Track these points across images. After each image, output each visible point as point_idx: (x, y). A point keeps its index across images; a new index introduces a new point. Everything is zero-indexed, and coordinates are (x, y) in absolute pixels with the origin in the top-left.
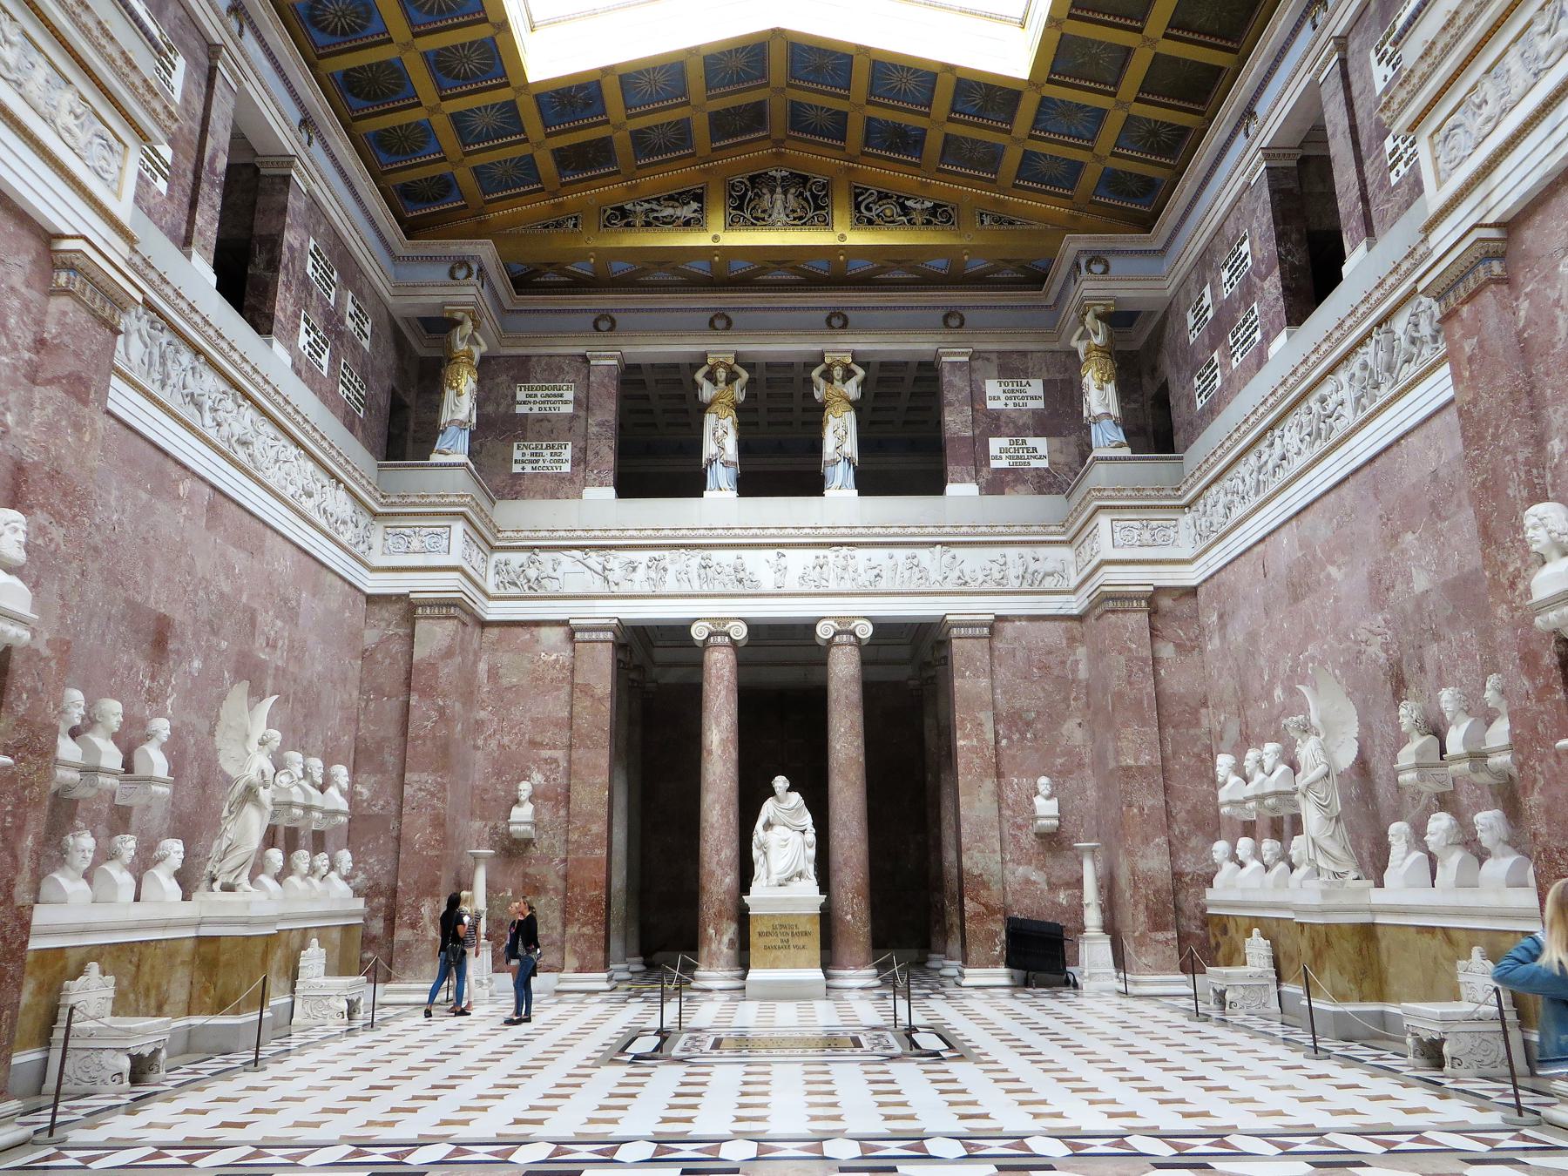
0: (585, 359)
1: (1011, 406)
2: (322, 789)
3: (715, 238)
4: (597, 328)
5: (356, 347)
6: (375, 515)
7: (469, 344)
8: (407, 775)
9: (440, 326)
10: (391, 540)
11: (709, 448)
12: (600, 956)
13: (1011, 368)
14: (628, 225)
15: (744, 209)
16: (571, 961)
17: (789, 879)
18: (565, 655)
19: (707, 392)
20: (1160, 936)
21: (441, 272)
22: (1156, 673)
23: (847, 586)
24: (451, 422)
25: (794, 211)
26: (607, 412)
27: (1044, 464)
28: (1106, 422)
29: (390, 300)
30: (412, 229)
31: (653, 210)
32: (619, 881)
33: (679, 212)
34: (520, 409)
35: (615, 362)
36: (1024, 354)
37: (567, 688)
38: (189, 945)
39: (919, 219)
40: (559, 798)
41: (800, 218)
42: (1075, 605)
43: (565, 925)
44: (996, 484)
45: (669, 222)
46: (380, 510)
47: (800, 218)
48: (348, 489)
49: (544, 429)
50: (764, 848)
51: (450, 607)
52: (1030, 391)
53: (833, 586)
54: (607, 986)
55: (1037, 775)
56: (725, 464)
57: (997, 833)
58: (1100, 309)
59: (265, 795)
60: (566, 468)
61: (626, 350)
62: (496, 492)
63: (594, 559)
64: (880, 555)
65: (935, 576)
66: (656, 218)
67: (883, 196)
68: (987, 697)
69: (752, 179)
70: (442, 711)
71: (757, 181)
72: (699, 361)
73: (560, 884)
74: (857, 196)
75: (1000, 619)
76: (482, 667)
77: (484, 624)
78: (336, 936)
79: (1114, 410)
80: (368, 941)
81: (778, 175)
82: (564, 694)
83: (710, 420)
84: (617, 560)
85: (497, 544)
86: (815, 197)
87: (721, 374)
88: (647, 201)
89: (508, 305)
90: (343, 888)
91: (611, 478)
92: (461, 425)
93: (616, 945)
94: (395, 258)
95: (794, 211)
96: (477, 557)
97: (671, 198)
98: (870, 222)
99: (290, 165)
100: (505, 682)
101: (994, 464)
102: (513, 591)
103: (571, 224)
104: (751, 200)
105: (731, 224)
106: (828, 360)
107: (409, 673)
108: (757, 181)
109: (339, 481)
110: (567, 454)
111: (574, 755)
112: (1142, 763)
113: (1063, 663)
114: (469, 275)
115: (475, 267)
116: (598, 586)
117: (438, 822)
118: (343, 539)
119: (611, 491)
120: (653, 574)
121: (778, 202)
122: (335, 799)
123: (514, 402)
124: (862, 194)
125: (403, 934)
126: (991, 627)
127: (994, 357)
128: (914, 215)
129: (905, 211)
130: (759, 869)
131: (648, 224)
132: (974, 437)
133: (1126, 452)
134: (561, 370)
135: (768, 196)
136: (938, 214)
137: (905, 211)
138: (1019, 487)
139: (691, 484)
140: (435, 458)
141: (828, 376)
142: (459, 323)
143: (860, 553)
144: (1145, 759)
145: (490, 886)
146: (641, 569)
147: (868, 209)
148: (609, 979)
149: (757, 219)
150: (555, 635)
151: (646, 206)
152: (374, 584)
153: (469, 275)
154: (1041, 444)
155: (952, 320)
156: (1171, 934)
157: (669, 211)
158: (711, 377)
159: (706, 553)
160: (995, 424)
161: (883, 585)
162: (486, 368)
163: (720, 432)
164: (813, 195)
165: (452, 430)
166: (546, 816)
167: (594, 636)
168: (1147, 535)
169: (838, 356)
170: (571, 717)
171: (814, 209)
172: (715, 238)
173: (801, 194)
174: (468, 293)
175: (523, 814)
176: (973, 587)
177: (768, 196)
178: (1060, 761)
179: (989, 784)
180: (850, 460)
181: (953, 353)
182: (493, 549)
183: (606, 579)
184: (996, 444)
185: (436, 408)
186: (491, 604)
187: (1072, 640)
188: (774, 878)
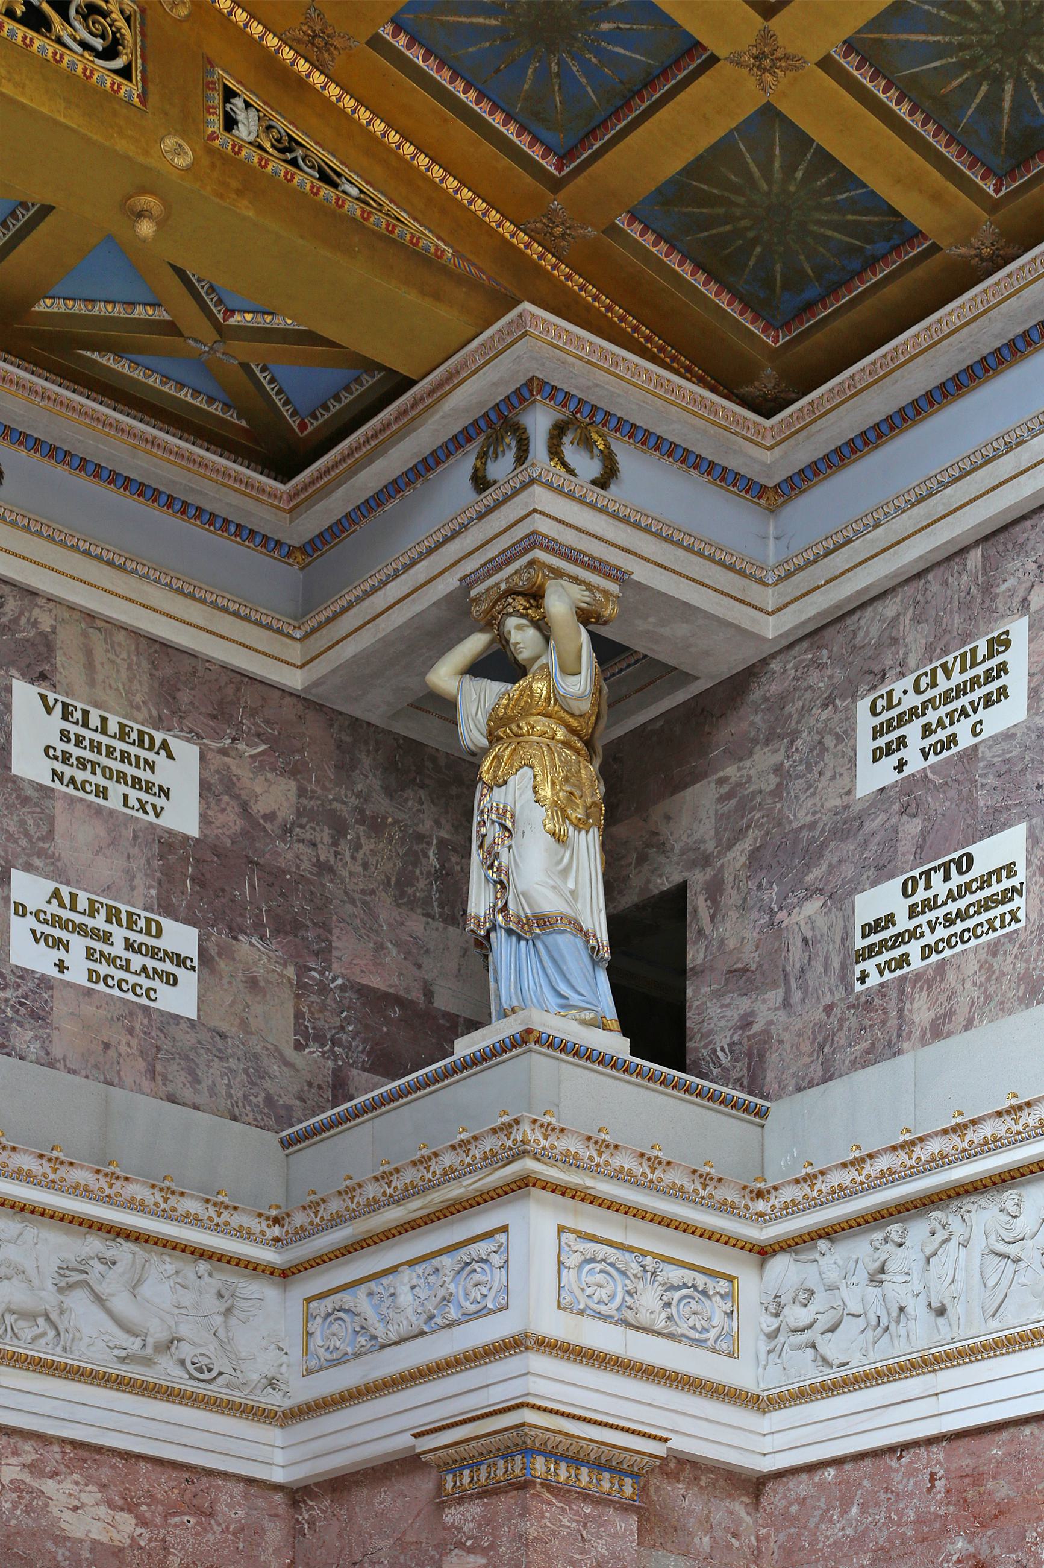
42: (279, 1457)
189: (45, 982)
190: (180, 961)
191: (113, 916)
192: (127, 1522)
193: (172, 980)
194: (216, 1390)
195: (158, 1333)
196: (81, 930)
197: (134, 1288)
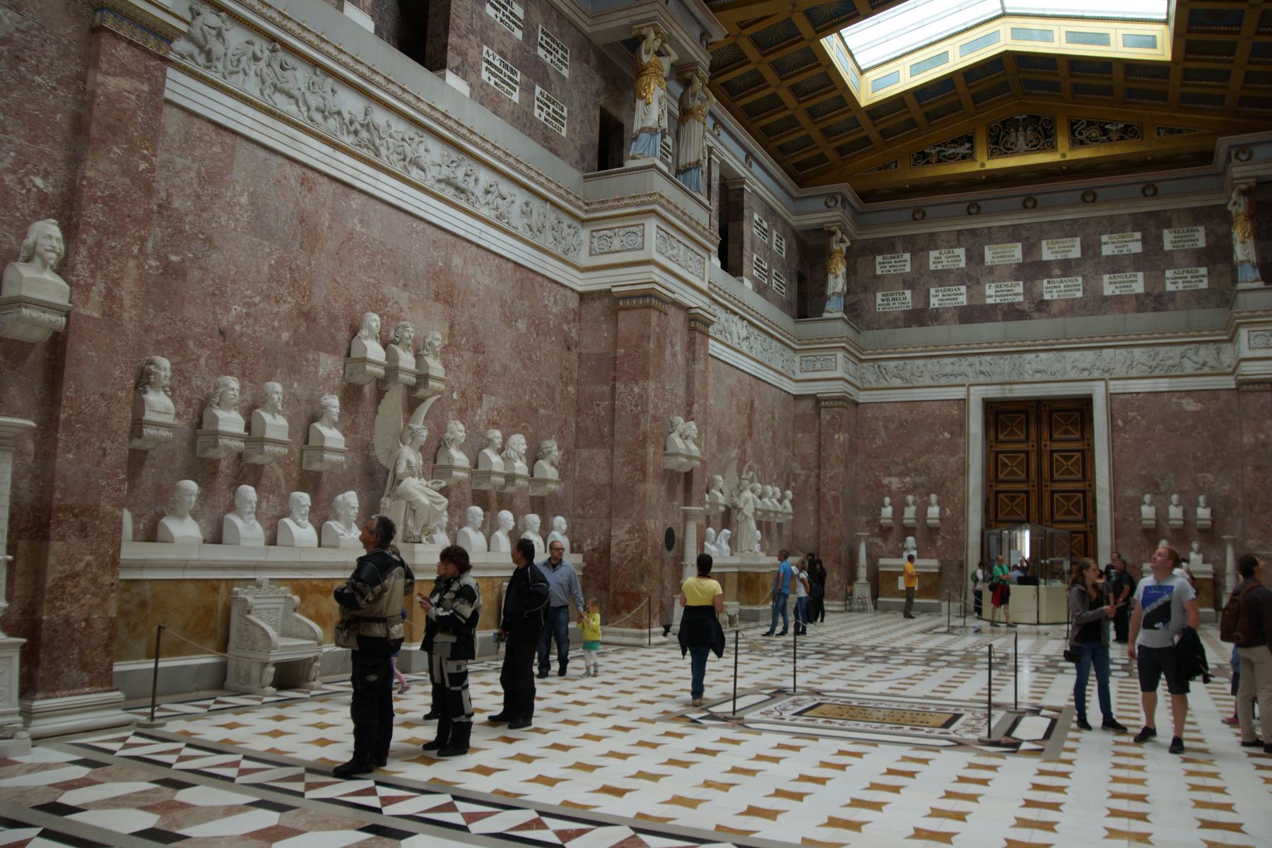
2: (760, 498)
3: (983, 165)
4: (915, 219)
7: (839, 246)
9: (824, 233)
14: (928, 163)
15: (999, 146)
21: (820, 203)
24: (833, 294)
25: (1031, 141)
28: (1247, 265)
29: (794, 224)
30: (801, 183)
31: (942, 151)
39: (1113, 136)
41: (1036, 146)
45: (952, 158)
46: (797, 347)
47: (1036, 146)
66: (944, 156)
67: (1090, 124)
69: (1003, 123)
71: (1008, 124)
74: (1072, 125)
79: (1253, 258)
81: (1020, 118)
85: (864, 357)
88: (939, 146)
92: (839, 295)
94: (794, 199)
95: (1031, 141)
96: (851, 366)
97: (953, 142)
98: (1082, 143)
99: (743, 182)
103: (893, 166)
104: (1003, 137)
105: (991, 155)
115: (839, 198)
124: (1076, 124)
128: (1111, 135)
129: (1105, 132)
131: (939, 161)
135: (1014, 134)
136: (1128, 132)
137: (1105, 132)
140: (826, 315)
142: (833, 234)
147: (1080, 134)
149: (1008, 149)
151: (938, 149)
152: (794, 389)
157: (952, 151)
162: (851, 257)
164: (1043, 128)
165: (834, 298)
171: (1045, 140)
173: (1036, 128)
177: (1014, 134)
182: (861, 361)
186: (862, 393)
189: (1174, 292)
190: (1203, 276)
191: (1188, 272)
192: (1200, 405)
193: (1201, 281)
194: (1216, 371)
195: (1201, 362)
196: (1181, 278)
197: (1196, 353)
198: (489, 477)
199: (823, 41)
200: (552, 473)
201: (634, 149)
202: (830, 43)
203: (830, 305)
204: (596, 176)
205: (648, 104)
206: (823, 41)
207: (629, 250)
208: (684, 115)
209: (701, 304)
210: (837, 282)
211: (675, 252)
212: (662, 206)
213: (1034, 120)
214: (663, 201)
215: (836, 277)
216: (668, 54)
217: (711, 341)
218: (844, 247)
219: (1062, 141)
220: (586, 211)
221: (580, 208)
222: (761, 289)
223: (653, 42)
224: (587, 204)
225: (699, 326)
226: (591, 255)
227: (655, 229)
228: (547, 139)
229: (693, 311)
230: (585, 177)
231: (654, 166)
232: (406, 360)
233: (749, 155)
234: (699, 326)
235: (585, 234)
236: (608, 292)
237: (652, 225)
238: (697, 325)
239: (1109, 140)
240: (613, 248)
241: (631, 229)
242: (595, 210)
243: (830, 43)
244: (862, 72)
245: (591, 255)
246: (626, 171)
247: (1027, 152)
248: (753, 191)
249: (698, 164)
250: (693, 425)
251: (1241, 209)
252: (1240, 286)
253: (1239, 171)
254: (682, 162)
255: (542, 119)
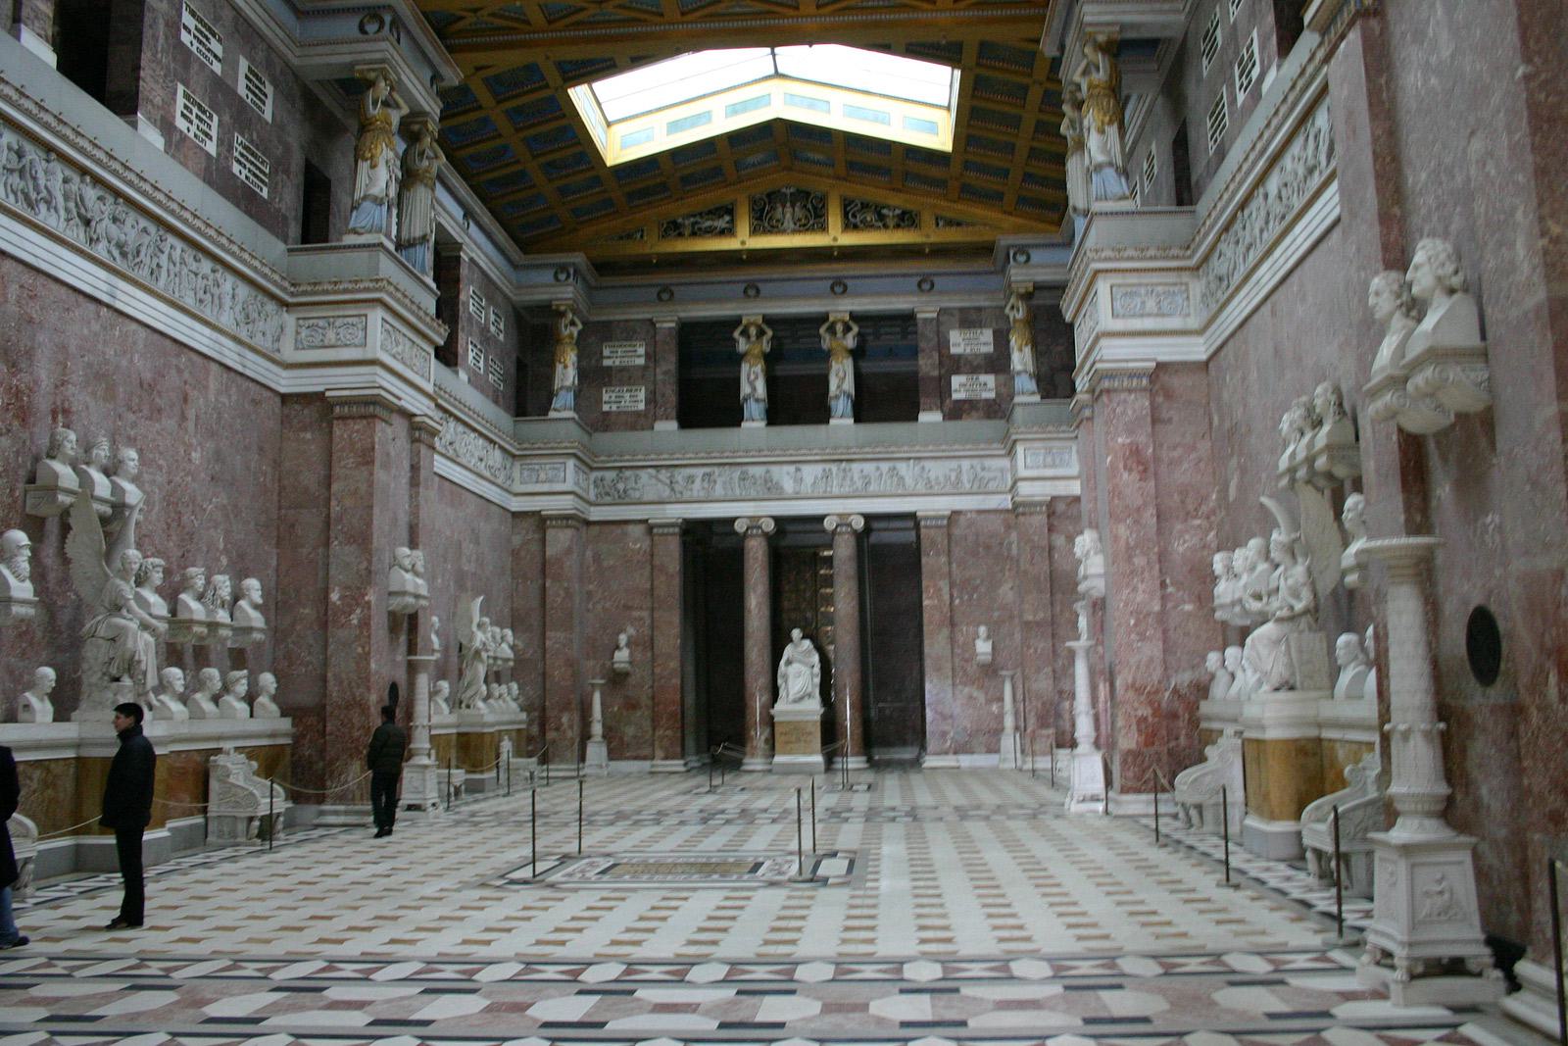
0: (652, 323)
1: (968, 351)
4: (660, 299)
5: (497, 341)
6: (514, 456)
7: (570, 331)
8: (548, 634)
10: (526, 473)
11: (745, 389)
12: (679, 749)
13: (969, 320)
14: (681, 235)
15: (763, 222)
16: (659, 753)
17: (801, 699)
18: (646, 544)
19: (742, 345)
20: (1045, 732)
21: (547, 276)
22: (1050, 556)
23: (846, 490)
24: (562, 388)
26: (669, 364)
27: (992, 395)
29: (514, 298)
30: (525, 247)
32: (690, 700)
33: (716, 224)
34: (607, 363)
35: (673, 325)
36: (979, 309)
37: (648, 568)
38: (454, 737)
39: (891, 223)
40: (645, 644)
43: (654, 729)
44: (956, 411)
45: (711, 232)
48: (501, 448)
49: (624, 377)
50: (785, 677)
51: (566, 519)
52: (983, 339)
53: (836, 491)
54: (683, 769)
55: (978, 625)
56: (757, 400)
57: (949, 665)
58: (1022, 291)
59: (484, 655)
60: (642, 406)
61: (683, 315)
62: (592, 426)
63: (664, 475)
64: (869, 467)
65: (909, 482)
68: (945, 569)
69: (769, 195)
70: (567, 590)
71: (773, 197)
72: (736, 322)
73: (650, 703)
74: (845, 207)
75: (954, 513)
76: (589, 554)
77: (588, 523)
78: (514, 734)
79: (1031, 368)
80: (530, 739)
81: (788, 191)
82: (647, 572)
83: (745, 368)
84: (680, 475)
86: (815, 208)
87: (753, 331)
88: (694, 216)
89: (593, 282)
90: (514, 705)
91: (674, 414)
92: (568, 389)
93: (690, 743)
94: (515, 266)
97: (710, 212)
98: (855, 227)
100: (605, 564)
101: (955, 396)
102: (608, 499)
105: (755, 231)
106: (831, 319)
107: (544, 565)
108: (773, 197)
109: (495, 443)
110: (642, 395)
111: (656, 615)
112: (1038, 618)
113: (1001, 544)
114: (568, 276)
116: (666, 493)
117: (570, 663)
118: (499, 481)
119: (673, 425)
120: (706, 485)
121: (787, 214)
122: (506, 651)
123: (602, 357)
125: (551, 735)
126: (949, 518)
127: (956, 313)
129: (881, 217)
130: (782, 693)
132: (940, 378)
133: (1037, 398)
134: (635, 332)
136: (907, 219)
137: (881, 217)
138: (974, 413)
139: (732, 416)
140: (552, 414)
141: (832, 330)
142: (562, 314)
143: (855, 466)
144: (1041, 615)
145: (603, 703)
146: (698, 481)
147: (854, 216)
148: (685, 765)
150: (637, 531)
152: (516, 505)
153: (568, 276)
154: (990, 380)
155: (925, 284)
156: (1051, 731)
158: (745, 333)
159: (745, 468)
160: (957, 364)
161: (872, 488)
162: (581, 343)
163: (752, 377)
166: (639, 656)
167: (666, 530)
168: (1049, 460)
169: (839, 316)
170: (652, 589)
171: (815, 220)
172: (743, 243)
174: (566, 293)
175: (622, 656)
176: (936, 489)
178: (996, 614)
179: (945, 632)
180: (849, 396)
181: (926, 308)
182: (592, 469)
183: (673, 490)
184: (957, 381)
185: (550, 378)
186: (592, 509)
187: (1008, 527)
188: (791, 697)
198: (189, 628)
199: (571, 92)
200: (257, 619)
201: (357, 220)
202: (579, 95)
203: (557, 403)
204: (301, 250)
205: (373, 167)
206: (571, 92)
207: (346, 345)
208: (408, 177)
209: (430, 413)
210: (567, 373)
211: (400, 348)
212: (390, 294)
213: (802, 196)
214: (391, 289)
215: (566, 367)
216: (398, 107)
217: (436, 457)
218: (575, 331)
219: (834, 220)
220: (292, 294)
221: (284, 289)
222: (475, 381)
223: (383, 91)
224: (293, 285)
225: (424, 436)
226: (297, 349)
227: (380, 321)
228: (243, 198)
229: (418, 419)
230: (290, 251)
231: (381, 245)
232: (102, 485)
233: (468, 214)
234: (424, 436)
235: (289, 319)
236: (319, 397)
237: (377, 315)
238: (419, 433)
239: (886, 226)
240: (326, 343)
241: (350, 320)
242: (305, 293)
243: (579, 95)
244: (609, 124)
245: (297, 349)
246: (340, 248)
247: (794, 232)
248: (472, 260)
249: (424, 239)
250: (419, 554)
251: (1020, 315)
252: (1017, 399)
253: (1020, 275)
254: (404, 235)
255: (243, 177)
